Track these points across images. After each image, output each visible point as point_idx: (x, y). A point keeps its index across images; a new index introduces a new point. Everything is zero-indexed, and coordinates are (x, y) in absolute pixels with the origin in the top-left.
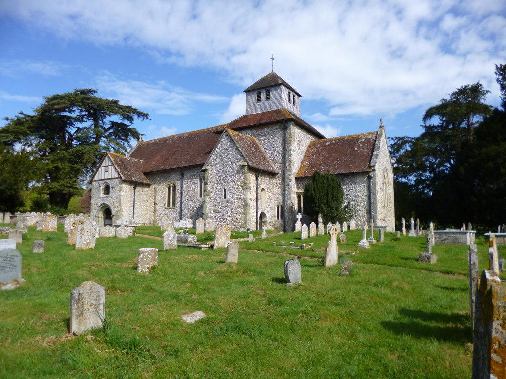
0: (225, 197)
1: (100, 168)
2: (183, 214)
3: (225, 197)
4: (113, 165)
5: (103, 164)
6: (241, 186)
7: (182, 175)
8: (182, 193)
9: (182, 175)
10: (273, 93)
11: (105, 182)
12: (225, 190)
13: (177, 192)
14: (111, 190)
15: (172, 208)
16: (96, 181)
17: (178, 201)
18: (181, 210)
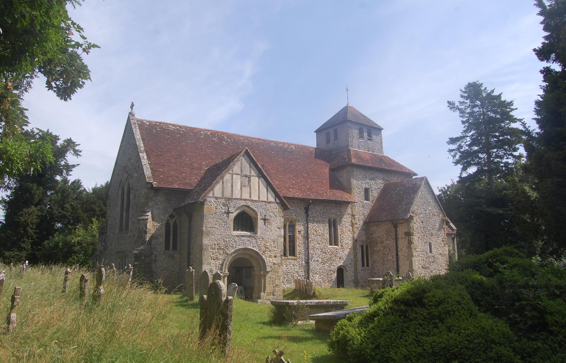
0: (431, 252)
1: (227, 177)
2: (311, 267)
3: (431, 252)
4: (261, 175)
5: (236, 168)
6: (443, 241)
7: (307, 210)
8: (307, 237)
9: (307, 210)
10: (374, 137)
11: (243, 206)
12: (430, 244)
13: (297, 235)
14: (260, 223)
15: (291, 259)
16: (216, 198)
17: (300, 247)
18: (308, 263)
